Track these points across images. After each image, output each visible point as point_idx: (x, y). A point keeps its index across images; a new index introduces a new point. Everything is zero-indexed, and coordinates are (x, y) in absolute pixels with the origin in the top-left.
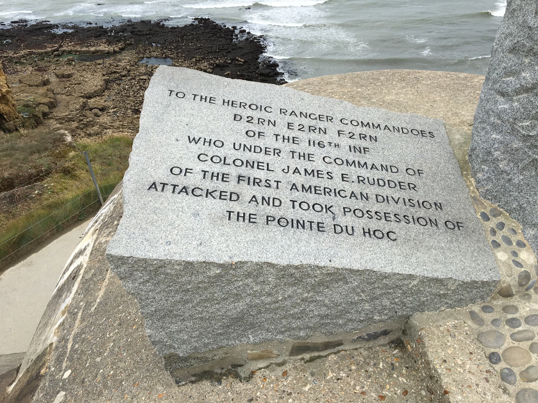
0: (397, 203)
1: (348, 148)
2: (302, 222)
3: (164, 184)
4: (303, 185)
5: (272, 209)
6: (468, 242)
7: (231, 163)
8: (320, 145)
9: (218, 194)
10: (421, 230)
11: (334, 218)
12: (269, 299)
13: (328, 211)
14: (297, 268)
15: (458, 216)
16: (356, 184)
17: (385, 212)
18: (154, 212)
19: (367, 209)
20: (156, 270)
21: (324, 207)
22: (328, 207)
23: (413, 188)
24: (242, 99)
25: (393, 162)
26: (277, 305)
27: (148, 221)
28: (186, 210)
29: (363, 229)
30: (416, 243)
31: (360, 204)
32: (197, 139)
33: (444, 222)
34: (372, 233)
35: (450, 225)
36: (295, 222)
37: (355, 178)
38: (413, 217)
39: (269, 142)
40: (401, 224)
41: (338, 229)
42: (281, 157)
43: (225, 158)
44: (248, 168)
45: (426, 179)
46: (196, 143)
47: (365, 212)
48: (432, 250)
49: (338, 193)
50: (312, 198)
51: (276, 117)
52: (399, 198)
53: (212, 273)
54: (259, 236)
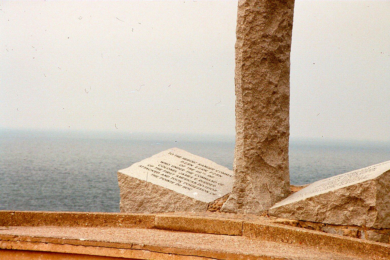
12: (149, 197)
14: (157, 186)
20: (126, 179)
26: (151, 200)
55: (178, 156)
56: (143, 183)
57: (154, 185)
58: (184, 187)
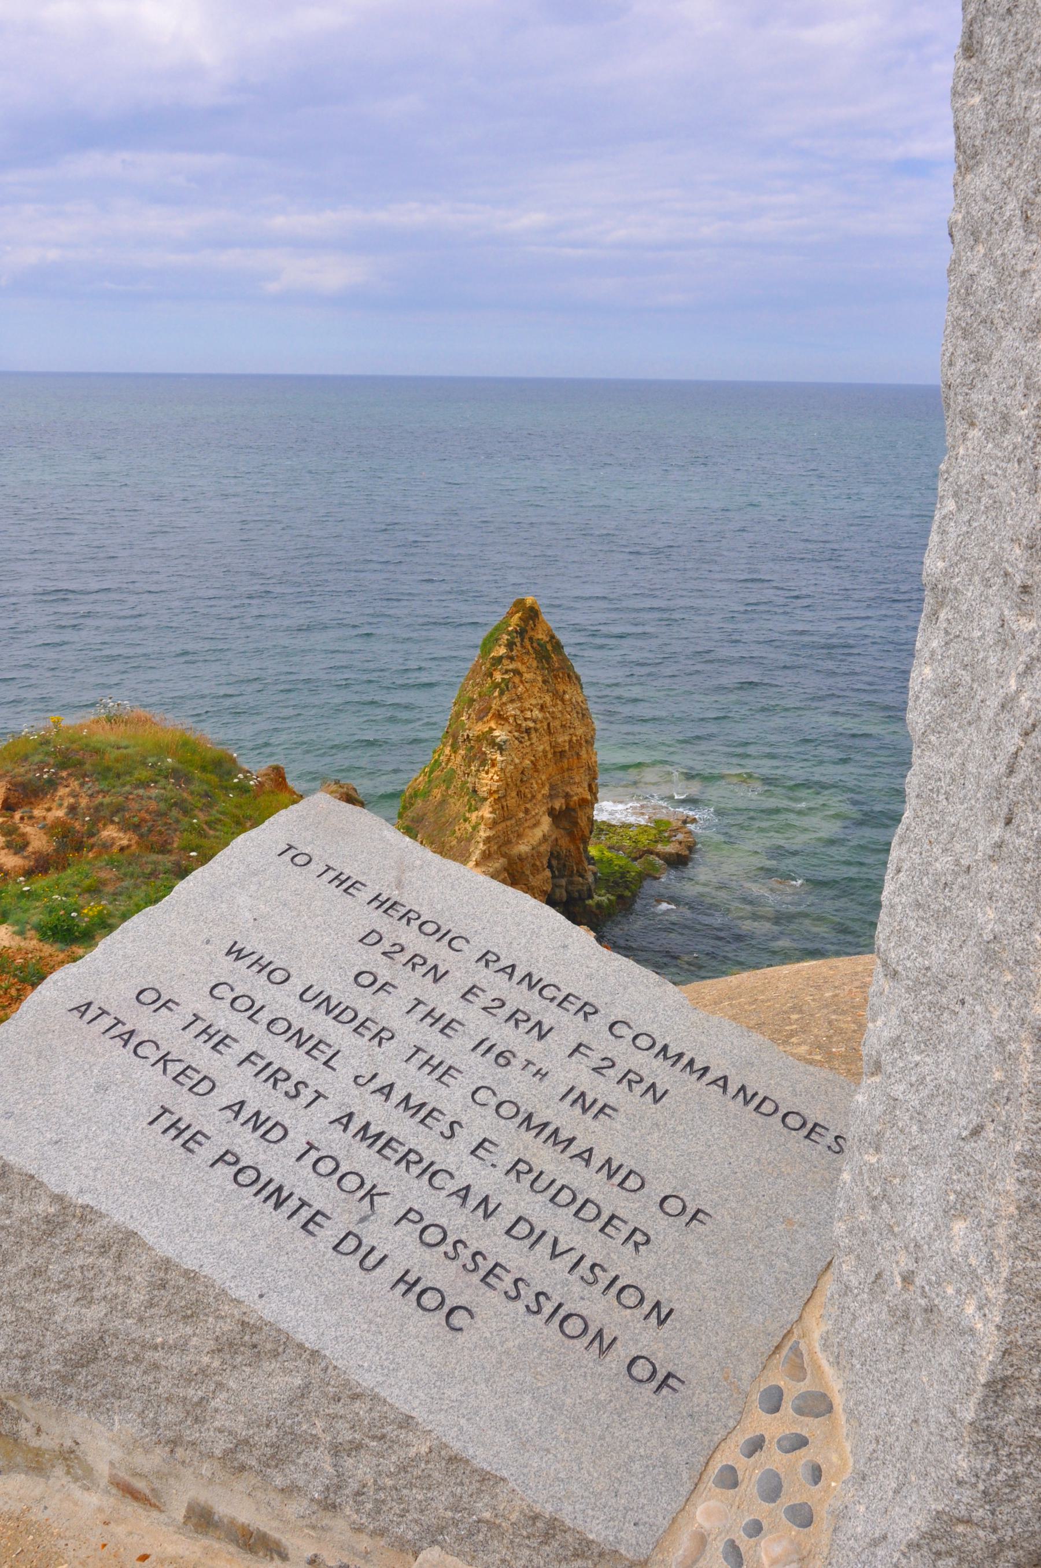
0: (554, 1255)
1: (564, 1090)
2: (285, 1194)
3: (104, 1012)
4: (368, 1124)
5: (252, 1143)
6: (646, 1430)
7: (266, 1021)
8: (504, 1058)
9: (179, 1067)
10: (549, 1344)
11: (363, 1220)
13: (368, 1199)
15: (693, 1360)
16: (499, 1173)
17: (503, 1262)
18: (40, 1052)
19: (463, 1237)
21: (368, 1186)
22: (374, 1192)
23: (636, 1245)
24: (421, 905)
25: (652, 1166)
27: (17, 1063)
28: (96, 1071)
29: (407, 1272)
30: (501, 1362)
31: (458, 1220)
32: (244, 953)
33: (634, 1353)
34: (418, 1289)
35: (641, 1370)
36: (271, 1188)
37: (509, 1160)
38: (560, 1305)
39: (389, 1010)
40: (511, 1305)
41: (353, 1246)
42: (382, 1050)
43: (263, 1007)
44: (287, 1045)
45: (699, 1239)
46: (237, 959)
47: (450, 1240)
48: (527, 1398)
49: (430, 1172)
50: (361, 1158)
51: (460, 965)
52: (572, 1249)
53: (40, 1208)
54: (174, 1179)
55: (339, 880)
56: (82, 1219)
57: (166, 1265)
58: (407, 1283)
